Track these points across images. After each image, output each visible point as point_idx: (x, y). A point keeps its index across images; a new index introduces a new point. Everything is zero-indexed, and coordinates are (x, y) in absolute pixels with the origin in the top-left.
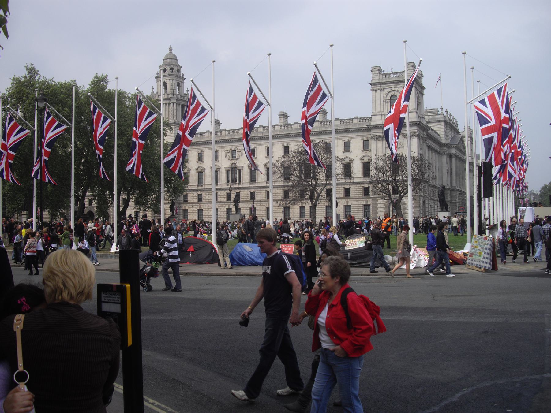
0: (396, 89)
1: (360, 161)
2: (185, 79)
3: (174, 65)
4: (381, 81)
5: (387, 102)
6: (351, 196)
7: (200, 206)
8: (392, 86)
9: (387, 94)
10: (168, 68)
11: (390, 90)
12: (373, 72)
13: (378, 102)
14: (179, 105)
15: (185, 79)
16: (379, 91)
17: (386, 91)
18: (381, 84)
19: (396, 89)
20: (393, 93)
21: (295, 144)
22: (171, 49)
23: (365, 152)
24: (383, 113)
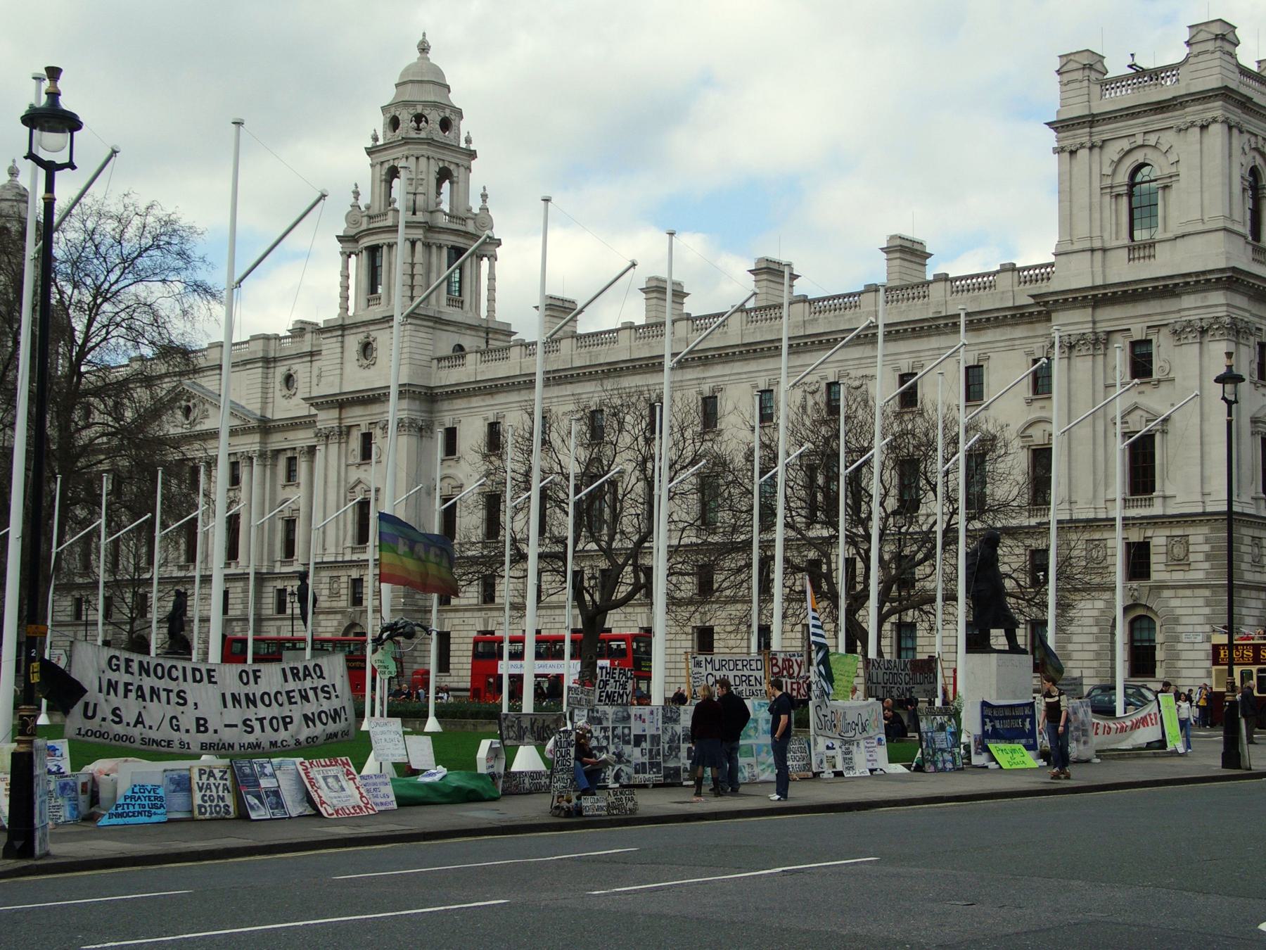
0: (1152, 139)
2: (472, 155)
3: (426, 104)
5: (1118, 196)
7: (486, 622)
8: (1135, 126)
10: (405, 116)
12: (1066, 77)
13: (1082, 198)
14: (440, 247)
15: (472, 155)
16: (1083, 153)
17: (1113, 151)
18: (1092, 120)
20: (1139, 157)
22: (424, 48)
23: (1037, 404)
24: (1097, 244)
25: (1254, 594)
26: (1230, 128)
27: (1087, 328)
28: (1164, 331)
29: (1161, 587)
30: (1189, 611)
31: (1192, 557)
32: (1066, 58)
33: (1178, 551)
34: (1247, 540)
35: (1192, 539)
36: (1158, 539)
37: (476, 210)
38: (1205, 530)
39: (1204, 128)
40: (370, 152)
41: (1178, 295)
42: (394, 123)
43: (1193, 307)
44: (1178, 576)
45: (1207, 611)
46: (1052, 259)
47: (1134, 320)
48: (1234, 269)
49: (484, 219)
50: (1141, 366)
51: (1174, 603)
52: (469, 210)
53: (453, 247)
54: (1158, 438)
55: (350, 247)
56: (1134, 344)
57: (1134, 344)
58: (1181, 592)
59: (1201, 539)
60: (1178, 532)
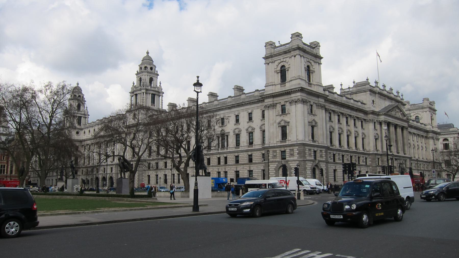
0: (285, 60)
1: (259, 130)
4: (274, 53)
6: (253, 162)
8: (281, 57)
9: (278, 66)
11: (279, 61)
14: (149, 94)
15: (158, 75)
16: (270, 64)
19: (285, 60)
20: (282, 64)
22: (148, 53)
23: (263, 121)
24: (273, 84)
25: (309, 162)
26: (301, 56)
27: (272, 103)
28: (288, 103)
29: (288, 161)
31: (295, 154)
32: (267, 43)
34: (307, 150)
35: (294, 150)
36: (288, 150)
37: (158, 86)
38: (297, 147)
39: (295, 56)
40: (136, 74)
41: (290, 94)
42: (141, 68)
43: (294, 96)
44: (292, 158)
46: (264, 88)
47: (281, 100)
48: (301, 87)
49: (160, 88)
50: (283, 110)
51: (291, 165)
52: (157, 86)
53: (152, 94)
54: (287, 127)
55: (132, 94)
56: (282, 106)
57: (282, 106)
59: (296, 150)
60: (291, 148)
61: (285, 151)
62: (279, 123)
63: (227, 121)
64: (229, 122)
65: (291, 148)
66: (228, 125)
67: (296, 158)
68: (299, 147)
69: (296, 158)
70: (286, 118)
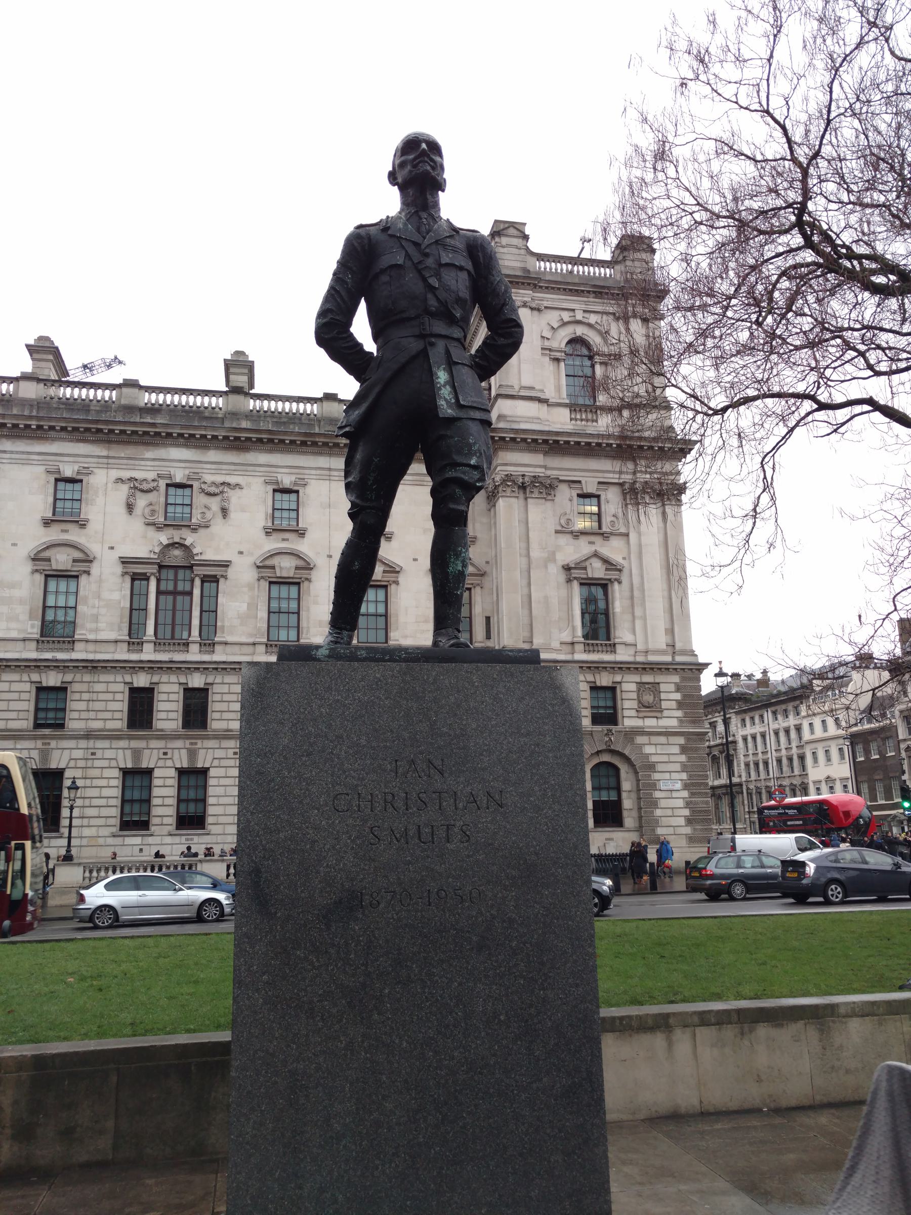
21: (115, 474)
30: (665, 758)
31: (664, 705)
33: (648, 698)
35: (663, 687)
36: (629, 685)
38: (676, 679)
44: (650, 723)
45: (683, 758)
51: (648, 750)
58: (655, 739)
59: (672, 687)
60: (648, 678)
61: (612, 690)
62: (581, 565)
63: (215, 504)
64: (225, 512)
65: (648, 678)
66: (218, 527)
67: (674, 723)
68: (683, 679)
69: (674, 723)
70: (613, 550)
